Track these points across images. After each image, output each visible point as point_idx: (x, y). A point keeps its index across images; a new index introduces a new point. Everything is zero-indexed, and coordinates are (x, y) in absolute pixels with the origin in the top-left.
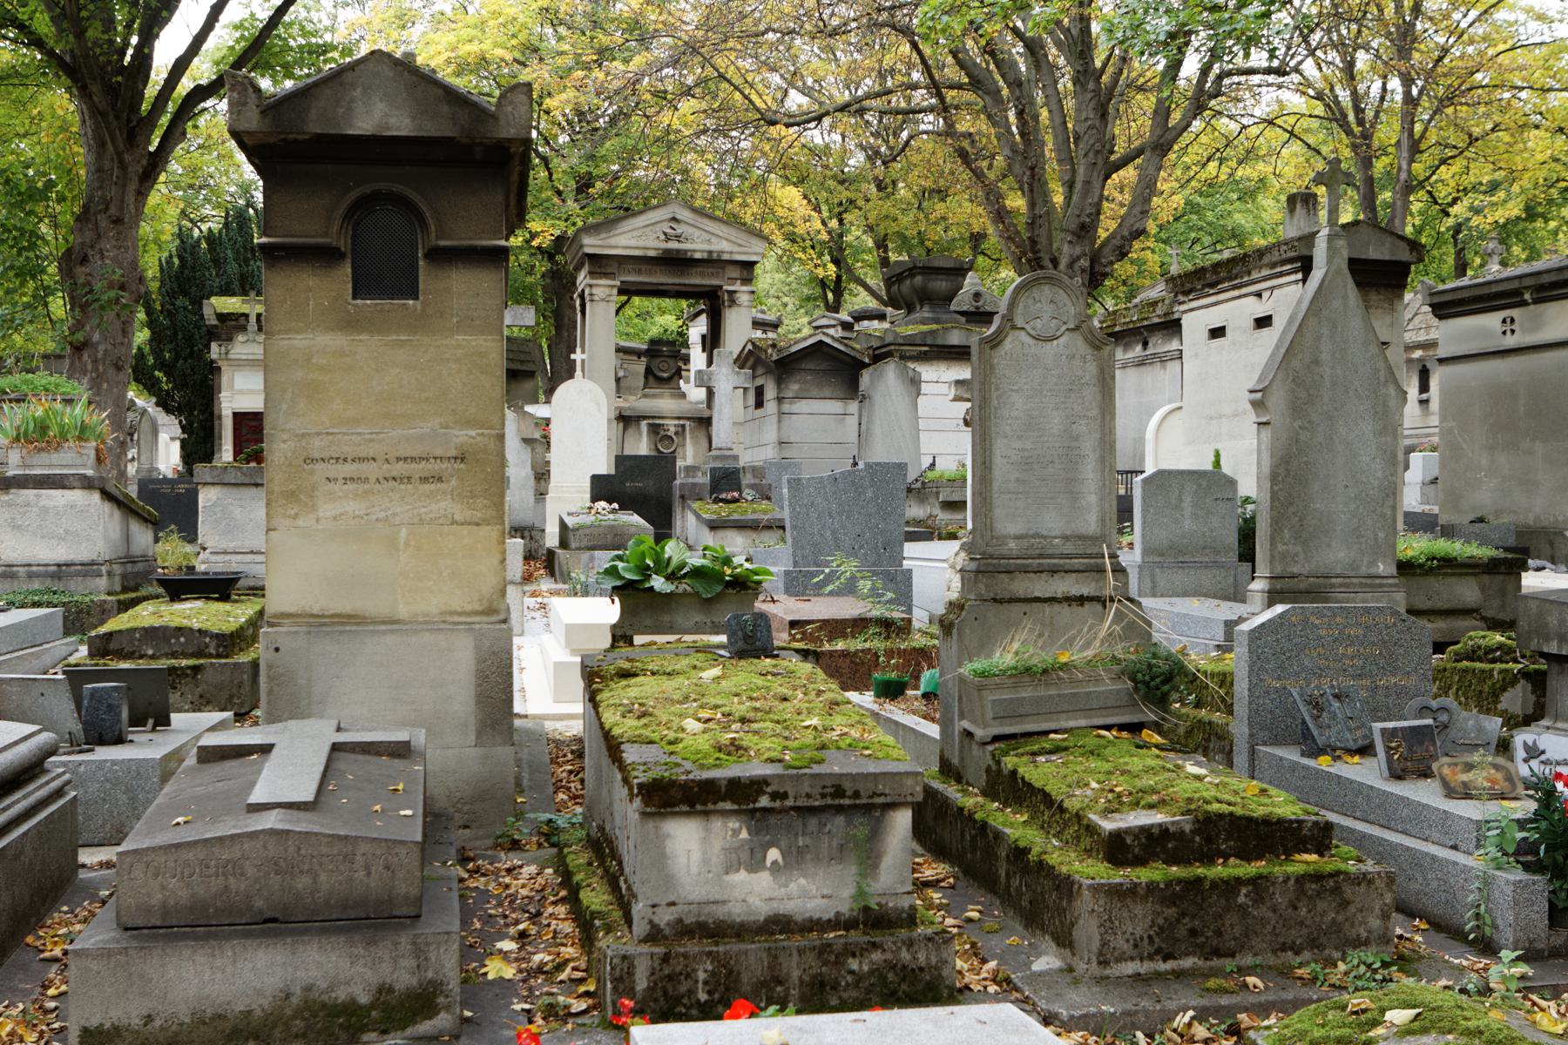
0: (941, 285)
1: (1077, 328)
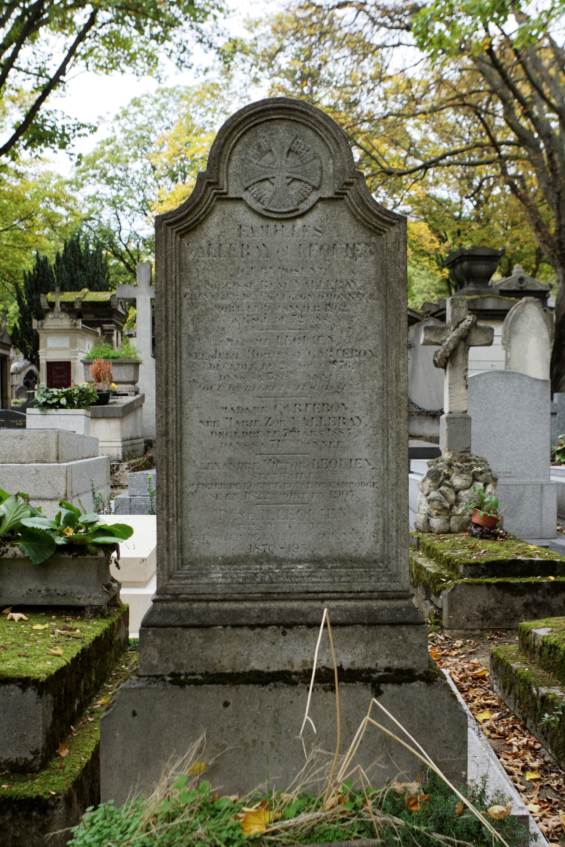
0: (481, 267)
1: (338, 198)
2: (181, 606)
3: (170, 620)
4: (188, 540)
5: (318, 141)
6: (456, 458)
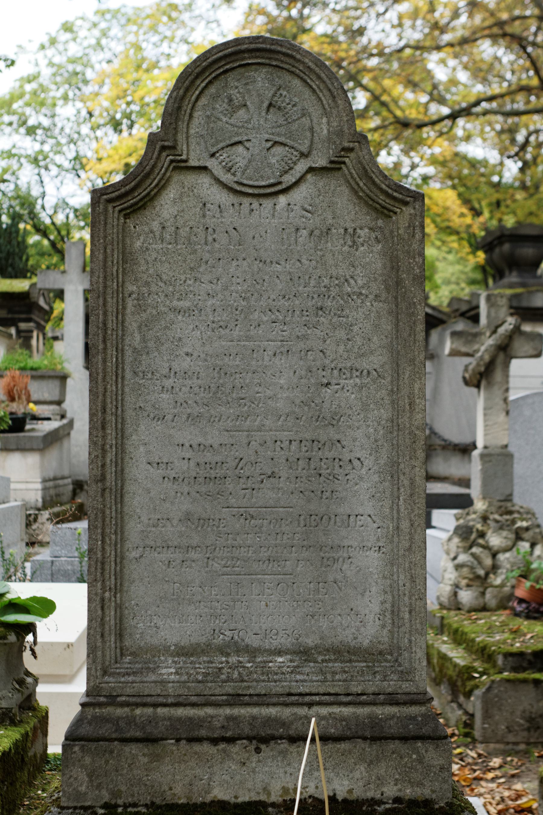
0: (528, 251)
1: (334, 167)
2: (120, 712)
3: (105, 730)
4: (130, 622)
5: (307, 93)
6: (493, 509)
